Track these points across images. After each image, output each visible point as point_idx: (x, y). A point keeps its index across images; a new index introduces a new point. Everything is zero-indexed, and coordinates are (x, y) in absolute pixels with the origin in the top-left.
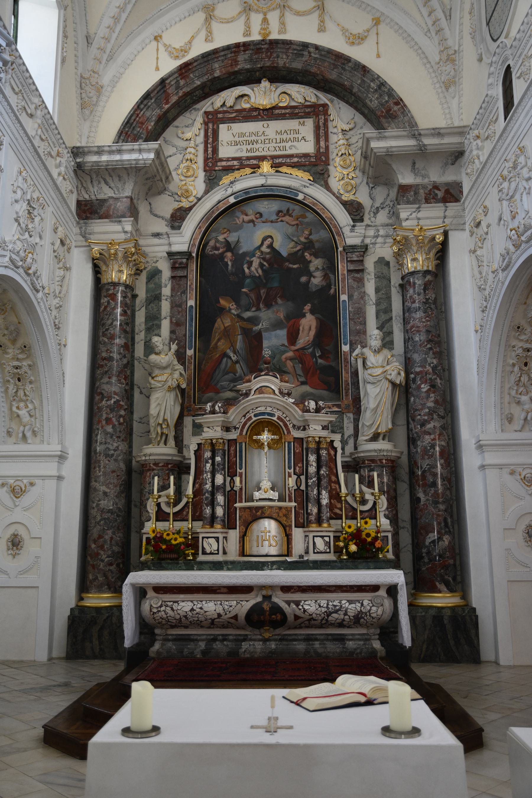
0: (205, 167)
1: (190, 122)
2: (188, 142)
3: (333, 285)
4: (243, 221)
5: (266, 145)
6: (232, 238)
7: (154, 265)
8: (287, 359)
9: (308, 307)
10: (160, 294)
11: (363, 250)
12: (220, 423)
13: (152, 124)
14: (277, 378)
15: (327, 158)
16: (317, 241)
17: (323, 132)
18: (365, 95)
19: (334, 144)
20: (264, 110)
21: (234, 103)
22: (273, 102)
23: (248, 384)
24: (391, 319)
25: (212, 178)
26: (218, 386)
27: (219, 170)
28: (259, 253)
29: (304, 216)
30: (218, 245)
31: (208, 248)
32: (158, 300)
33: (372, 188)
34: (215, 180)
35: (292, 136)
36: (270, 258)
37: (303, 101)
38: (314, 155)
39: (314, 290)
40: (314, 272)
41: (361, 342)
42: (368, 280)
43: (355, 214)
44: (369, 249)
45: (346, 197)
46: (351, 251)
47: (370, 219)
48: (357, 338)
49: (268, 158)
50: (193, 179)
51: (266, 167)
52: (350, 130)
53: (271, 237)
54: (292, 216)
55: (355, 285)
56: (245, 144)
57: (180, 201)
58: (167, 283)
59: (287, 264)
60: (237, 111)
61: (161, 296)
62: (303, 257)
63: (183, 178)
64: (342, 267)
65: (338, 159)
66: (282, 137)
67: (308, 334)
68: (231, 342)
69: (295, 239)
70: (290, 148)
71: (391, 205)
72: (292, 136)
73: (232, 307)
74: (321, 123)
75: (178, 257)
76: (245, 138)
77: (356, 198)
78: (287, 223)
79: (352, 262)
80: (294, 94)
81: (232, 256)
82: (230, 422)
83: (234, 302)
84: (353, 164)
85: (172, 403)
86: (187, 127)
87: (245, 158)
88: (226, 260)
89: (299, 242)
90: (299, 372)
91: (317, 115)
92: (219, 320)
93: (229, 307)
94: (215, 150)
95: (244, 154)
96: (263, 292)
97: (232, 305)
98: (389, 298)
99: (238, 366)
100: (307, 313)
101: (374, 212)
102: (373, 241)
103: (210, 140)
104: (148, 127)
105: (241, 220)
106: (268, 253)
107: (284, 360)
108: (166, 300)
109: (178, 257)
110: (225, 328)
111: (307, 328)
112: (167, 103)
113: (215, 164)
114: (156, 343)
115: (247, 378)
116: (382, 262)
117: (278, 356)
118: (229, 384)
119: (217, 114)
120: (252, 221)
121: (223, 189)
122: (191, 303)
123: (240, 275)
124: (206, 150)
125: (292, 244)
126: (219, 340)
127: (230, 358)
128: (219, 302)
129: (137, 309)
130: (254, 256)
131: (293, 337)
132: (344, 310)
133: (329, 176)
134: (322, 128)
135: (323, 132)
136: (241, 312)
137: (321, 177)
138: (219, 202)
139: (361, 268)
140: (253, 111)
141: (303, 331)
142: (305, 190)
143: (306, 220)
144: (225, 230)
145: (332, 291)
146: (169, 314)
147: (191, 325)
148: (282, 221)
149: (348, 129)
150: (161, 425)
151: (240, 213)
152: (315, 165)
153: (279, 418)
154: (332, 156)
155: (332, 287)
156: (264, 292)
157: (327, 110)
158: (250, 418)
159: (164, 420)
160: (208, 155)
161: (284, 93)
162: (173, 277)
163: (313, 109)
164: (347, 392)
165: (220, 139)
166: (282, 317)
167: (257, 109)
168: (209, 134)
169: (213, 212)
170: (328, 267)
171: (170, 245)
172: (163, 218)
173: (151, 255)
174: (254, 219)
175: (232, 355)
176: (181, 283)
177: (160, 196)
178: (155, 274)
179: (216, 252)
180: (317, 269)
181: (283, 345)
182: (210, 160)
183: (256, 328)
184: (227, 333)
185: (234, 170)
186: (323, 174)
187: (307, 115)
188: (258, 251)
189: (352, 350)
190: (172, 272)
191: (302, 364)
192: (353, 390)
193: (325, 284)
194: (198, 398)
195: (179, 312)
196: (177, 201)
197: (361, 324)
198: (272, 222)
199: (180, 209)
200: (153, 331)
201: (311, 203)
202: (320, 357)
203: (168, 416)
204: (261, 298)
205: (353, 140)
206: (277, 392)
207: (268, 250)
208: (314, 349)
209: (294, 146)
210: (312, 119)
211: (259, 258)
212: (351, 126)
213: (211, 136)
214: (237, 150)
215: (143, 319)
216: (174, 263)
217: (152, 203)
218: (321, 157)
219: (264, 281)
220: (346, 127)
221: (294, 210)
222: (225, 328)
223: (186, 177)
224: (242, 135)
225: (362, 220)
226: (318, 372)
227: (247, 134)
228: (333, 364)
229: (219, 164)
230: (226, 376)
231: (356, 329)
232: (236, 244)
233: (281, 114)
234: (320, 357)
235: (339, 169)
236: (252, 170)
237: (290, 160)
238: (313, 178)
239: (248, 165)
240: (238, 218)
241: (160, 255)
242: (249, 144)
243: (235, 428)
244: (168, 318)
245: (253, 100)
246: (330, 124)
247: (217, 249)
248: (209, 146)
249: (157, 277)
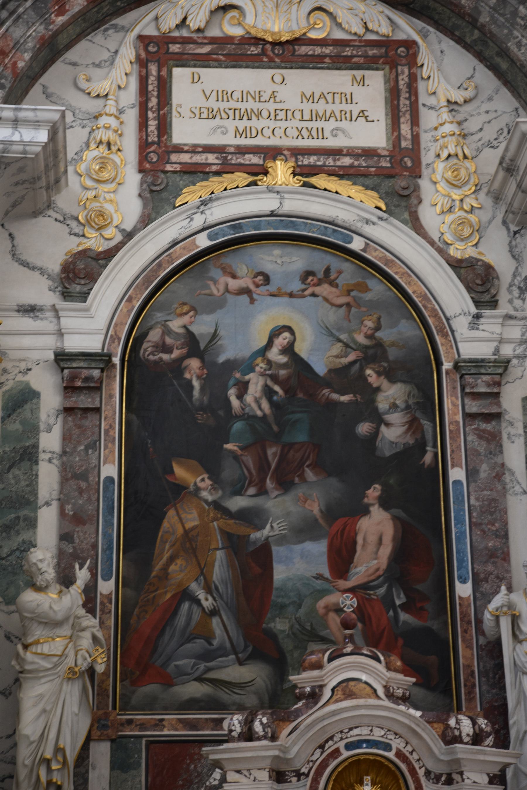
0: (141, 163)
1: (106, 55)
2: (100, 102)
3: (430, 443)
4: (227, 290)
5: (279, 123)
7: (20, 378)
10: (36, 446)
11: (500, 371)
12: (267, 763)
13: (27, 56)
14: (379, 661)
16: (393, 344)
17: (408, 102)
18: (506, 31)
19: (430, 130)
20: (274, 44)
21: (207, 22)
22: (295, 27)
23: (315, 673)
25: (155, 188)
26: (171, 669)
28: (262, 365)
29: (365, 289)
30: (169, 341)
31: (145, 345)
32: (30, 460)
33: (516, 233)
34: (165, 195)
35: (337, 108)
36: (288, 378)
37: (361, 31)
38: (386, 153)
39: (388, 453)
40: (387, 412)
41: (498, 577)
42: (509, 438)
43: (480, 289)
44: (510, 369)
46: (473, 371)
47: (510, 301)
48: (490, 568)
49: (286, 152)
50: (112, 186)
52: (465, 102)
53: (289, 329)
54: (337, 286)
55: (482, 447)
56: (232, 117)
57: (83, 236)
58: (52, 421)
59: (326, 391)
60: (213, 41)
61: (37, 452)
62: (363, 378)
63: (89, 183)
65: (440, 166)
66: (315, 107)
67: (377, 552)
68: (199, 564)
69: (343, 337)
70: (334, 133)
73: (201, 485)
74: (401, 83)
75: (82, 364)
76: (232, 104)
77: (480, 253)
78: (326, 299)
79: (476, 396)
80: (342, 16)
81: (202, 368)
82: (288, 761)
83: (208, 472)
84: (474, 180)
85: (76, 709)
86: (98, 66)
87: (232, 150)
88: (187, 376)
89: (352, 345)
91: (393, 65)
92: (171, 513)
93: (195, 484)
97: (203, 480)
99: (215, 621)
100: (373, 505)
101: (519, 288)
103: (153, 102)
104: (15, 63)
105: (222, 288)
106: (284, 366)
107: (321, 611)
108: (50, 461)
109: (82, 364)
110: (186, 532)
111: (372, 539)
112: (61, 12)
113: (164, 158)
114: (40, 565)
115: (313, 658)
117: (307, 602)
118: (195, 665)
119: (167, 44)
120: (246, 291)
121: (184, 216)
123: (221, 413)
124: (143, 124)
125: (337, 349)
126: (172, 559)
127: (198, 602)
128: (172, 472)
130: (252, 370)
132: (459, 501)
133: (420, 202)
134: (404, 95)
135: (408, 102)
136: (222, 497)
137: (404, 204)
138: (175, 243)
139: (494, 410)
140: (250, 44)
141: (363, 546)
142: (369, 230)
143: (368, 296)
144: (186, 308)
145: (428, 458)
146: (55, 495)
148: (313, 295)
149: (460, 100)
150: (48, 762)
151: (219, 272)
153: (399, 754)
154: (427, 158)
155: (428, 448)
156: (275, 454)
157: (415, 56)
158: (336, 753)
159: (58, 750)
160: (147, 135)
161: (320, 9)
162: (68, 411)
163: (383, 50)
164: (470, 692)
165: (175, 101)
166: (316, 511)
167: (257, 41)
168: (150, 88)
169: (160, 265)
170: (417, 403)
171: (60, 334)
172: (42, 271)
173: (12, 354)
174: (252, 287)
175: (201, 595)
176: (87, 423)
177: (34, 221)
179: (165, 357)
180: (394, 407)
181: (319, 577)
182: (153, 148)
183: (257, 536)
185: (208, 173)
186: (408, 196)
188: (259, 360)
190: (66, 397)
192: (484, 688)
193: (411, 442)
194: (122, 695)
195: (81, 492)
196: (76, 235)
197: (497, 536)
198: (291, 295)
199: (84, 254)
200: (18, 533)
201: (380, 259)
202: (403, 607)
203: (66, 742)
204: (269, 467)
205: (472, 125)
206: (381, 692)
207: (283, 359)
208: (389, 589)
209: (343, 131)
210: (381, 73)
211: (262, 374)
212: (468, 94)
213: (155, 93)
216: (73, 378)
217: (16, 234)
218: (402, 160)
219: (275, 428)
220: (458, 96)
221: (340, 272)
222: (186, 532)
223: (98, 181)
225: (493, 304)
226: (400, 642)
228: (435, 625)
229: (174, 157)
230: (189, 646)
231: (486, 548)
233: (312, 56)
234: (403, 607)
235: (442, 187)
236: (251, 179)
237: (334, 160)
238: (386, 204)
240: (215, 282)
241: (35, 355)
242: (241, 119)
243: (299, 775)
244: (55, 505)
245: (250, 20)
246: (421, 86)
247: (168, 350)
248: (150, 115)
249: (27, 406)
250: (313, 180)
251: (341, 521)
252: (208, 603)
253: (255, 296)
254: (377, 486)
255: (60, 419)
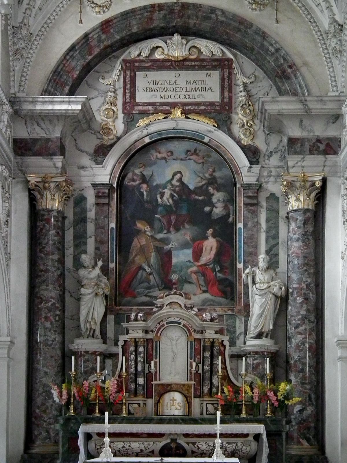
0: (123, 110)
4: (157, 158)
5: (177, 93)
6: (147, 172)
7: (80, 192)
8: (191, 272)
9: (210, 232)
10: (86, 217)
11: (258, 188)
15: (230, 107)
16: (220, 178)
17: (228, 84)
20: (175, 61)
24: (278, 243)
27: (136, 114)
30: (135, 177)
31: (126, 179)
33: (268, 134)
35: (200, 86)
38: (218, 104)
39: (216, 218)
40: (216, 203)
45: (245, 141)
46: (247, 188)
49: (179, 105)
51: (178, 112)
52: (250, 83)
53: (180, 173)
54: (199, 156)
55: (249, 215)
56: (159, 91)
57: (102, 139)
58: (91, 208)
61: (86, 219)
62: (207, 190)
64: (240, 201)
67: (210, 253)
69: (201, 175)
70: (199, 96)
71: (283, 150)
72: (200, 86)
73: (146, 230)
74: (225, 76)
76: (159, 86)
80: (203, 49)
87: (158, 104)
88: (142, 190)
89: (204, 178)
90: (202, 283)
91: (223, 69)
92: (136, 240)
93: (145, 229)
94: (133, 96)
95: (158, 100)
96: (173, 218)
98: (277, 227)
99: (151, 277)
100: (209, 236)
101: (268, 156)
102: (266, 180)
105: (155, 157)
106: (177, 186)
107: (189, 273)
110: (141, 246)
111: (209, 248)
116: (273, 197)
117: (184, 270)
120: (164, 158)
121: (140, 131)
122: (113, 225)
124: (124, 95)
126: (136, 256)
127: (145, 270)
129: (66, 229)
131: (197, 255)
132: (240, 235)
133: (231, 123)
134: (226, 81)
138: (136, 141)
139: (255, 201)
142: (210, 135)
144: (141, 165)
145: (231, 220)
146: (94, 234)
147: (112, 244)
148: (190, 159)
149: (249, 82)
152: (219, 112)
155: (231, 216)
156: (174, 218)
165: (137, 85)
166: (189, 239)
169: (131, 150)
172: (87, 153)
174: (166, 157)
175: (146, 268)
178: (81, 200)
179: (134, 184)
180: (219, 200)
181: (189, 261)
182: (128, 104)
184: (143, 250)
185: (149, 114)
186: (226, 121)
187: (214, 68)
188: (169, 184)
189: (245, 267)
191: (204, 277)
195: (102, 233)
196: (99, 139)
198: (181, 160)
202: (219, 271)
204: (172, 223)
207: (178, 184)
208: (214, 265)
209: (202, 95)
211: (170, 190)
214: (152, 96)
215: (72, 238)
218: (225, 106)
219: (174, 209)
221: (200, 150)
222: (141, 246)
224: (156, 82)
225: (257, 163)
227: (161, 82)
229: (136, 108)
232: (151, 177)
233: (191, 66)
234: (219, 271)
236: (166, 116)
237: (198, 107)
238: (217, 124)
239: (161, 110)
240: (152, 155)
242: (162, 91)
244: (93, 238)
247: (134, 181)
248: (127, 91)
250: (189, 116)
251: (198, 242)
252: (148, 270)
253: (168, 160)
254: (211, 229)
255: (94, 207)
